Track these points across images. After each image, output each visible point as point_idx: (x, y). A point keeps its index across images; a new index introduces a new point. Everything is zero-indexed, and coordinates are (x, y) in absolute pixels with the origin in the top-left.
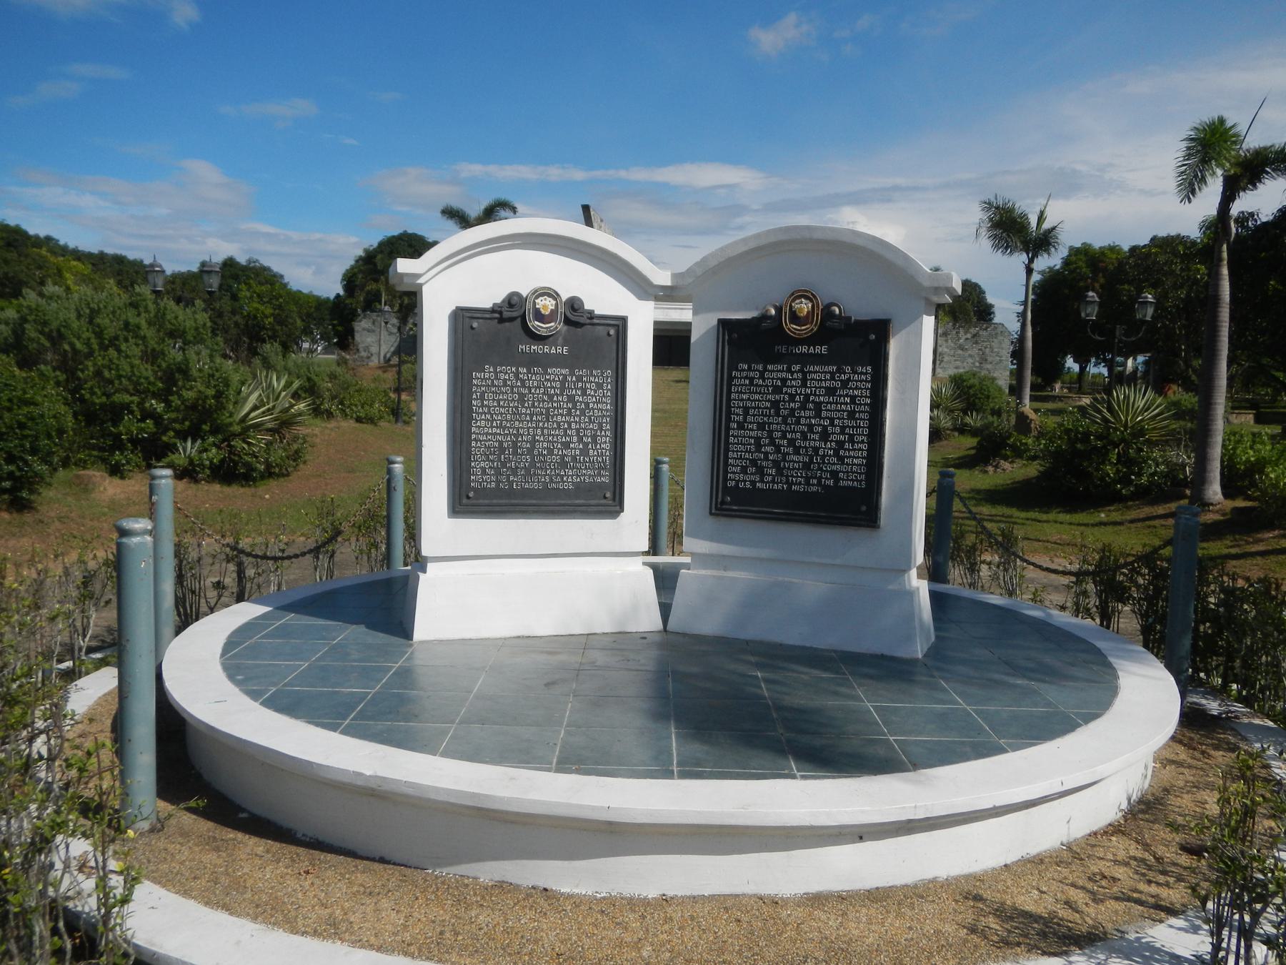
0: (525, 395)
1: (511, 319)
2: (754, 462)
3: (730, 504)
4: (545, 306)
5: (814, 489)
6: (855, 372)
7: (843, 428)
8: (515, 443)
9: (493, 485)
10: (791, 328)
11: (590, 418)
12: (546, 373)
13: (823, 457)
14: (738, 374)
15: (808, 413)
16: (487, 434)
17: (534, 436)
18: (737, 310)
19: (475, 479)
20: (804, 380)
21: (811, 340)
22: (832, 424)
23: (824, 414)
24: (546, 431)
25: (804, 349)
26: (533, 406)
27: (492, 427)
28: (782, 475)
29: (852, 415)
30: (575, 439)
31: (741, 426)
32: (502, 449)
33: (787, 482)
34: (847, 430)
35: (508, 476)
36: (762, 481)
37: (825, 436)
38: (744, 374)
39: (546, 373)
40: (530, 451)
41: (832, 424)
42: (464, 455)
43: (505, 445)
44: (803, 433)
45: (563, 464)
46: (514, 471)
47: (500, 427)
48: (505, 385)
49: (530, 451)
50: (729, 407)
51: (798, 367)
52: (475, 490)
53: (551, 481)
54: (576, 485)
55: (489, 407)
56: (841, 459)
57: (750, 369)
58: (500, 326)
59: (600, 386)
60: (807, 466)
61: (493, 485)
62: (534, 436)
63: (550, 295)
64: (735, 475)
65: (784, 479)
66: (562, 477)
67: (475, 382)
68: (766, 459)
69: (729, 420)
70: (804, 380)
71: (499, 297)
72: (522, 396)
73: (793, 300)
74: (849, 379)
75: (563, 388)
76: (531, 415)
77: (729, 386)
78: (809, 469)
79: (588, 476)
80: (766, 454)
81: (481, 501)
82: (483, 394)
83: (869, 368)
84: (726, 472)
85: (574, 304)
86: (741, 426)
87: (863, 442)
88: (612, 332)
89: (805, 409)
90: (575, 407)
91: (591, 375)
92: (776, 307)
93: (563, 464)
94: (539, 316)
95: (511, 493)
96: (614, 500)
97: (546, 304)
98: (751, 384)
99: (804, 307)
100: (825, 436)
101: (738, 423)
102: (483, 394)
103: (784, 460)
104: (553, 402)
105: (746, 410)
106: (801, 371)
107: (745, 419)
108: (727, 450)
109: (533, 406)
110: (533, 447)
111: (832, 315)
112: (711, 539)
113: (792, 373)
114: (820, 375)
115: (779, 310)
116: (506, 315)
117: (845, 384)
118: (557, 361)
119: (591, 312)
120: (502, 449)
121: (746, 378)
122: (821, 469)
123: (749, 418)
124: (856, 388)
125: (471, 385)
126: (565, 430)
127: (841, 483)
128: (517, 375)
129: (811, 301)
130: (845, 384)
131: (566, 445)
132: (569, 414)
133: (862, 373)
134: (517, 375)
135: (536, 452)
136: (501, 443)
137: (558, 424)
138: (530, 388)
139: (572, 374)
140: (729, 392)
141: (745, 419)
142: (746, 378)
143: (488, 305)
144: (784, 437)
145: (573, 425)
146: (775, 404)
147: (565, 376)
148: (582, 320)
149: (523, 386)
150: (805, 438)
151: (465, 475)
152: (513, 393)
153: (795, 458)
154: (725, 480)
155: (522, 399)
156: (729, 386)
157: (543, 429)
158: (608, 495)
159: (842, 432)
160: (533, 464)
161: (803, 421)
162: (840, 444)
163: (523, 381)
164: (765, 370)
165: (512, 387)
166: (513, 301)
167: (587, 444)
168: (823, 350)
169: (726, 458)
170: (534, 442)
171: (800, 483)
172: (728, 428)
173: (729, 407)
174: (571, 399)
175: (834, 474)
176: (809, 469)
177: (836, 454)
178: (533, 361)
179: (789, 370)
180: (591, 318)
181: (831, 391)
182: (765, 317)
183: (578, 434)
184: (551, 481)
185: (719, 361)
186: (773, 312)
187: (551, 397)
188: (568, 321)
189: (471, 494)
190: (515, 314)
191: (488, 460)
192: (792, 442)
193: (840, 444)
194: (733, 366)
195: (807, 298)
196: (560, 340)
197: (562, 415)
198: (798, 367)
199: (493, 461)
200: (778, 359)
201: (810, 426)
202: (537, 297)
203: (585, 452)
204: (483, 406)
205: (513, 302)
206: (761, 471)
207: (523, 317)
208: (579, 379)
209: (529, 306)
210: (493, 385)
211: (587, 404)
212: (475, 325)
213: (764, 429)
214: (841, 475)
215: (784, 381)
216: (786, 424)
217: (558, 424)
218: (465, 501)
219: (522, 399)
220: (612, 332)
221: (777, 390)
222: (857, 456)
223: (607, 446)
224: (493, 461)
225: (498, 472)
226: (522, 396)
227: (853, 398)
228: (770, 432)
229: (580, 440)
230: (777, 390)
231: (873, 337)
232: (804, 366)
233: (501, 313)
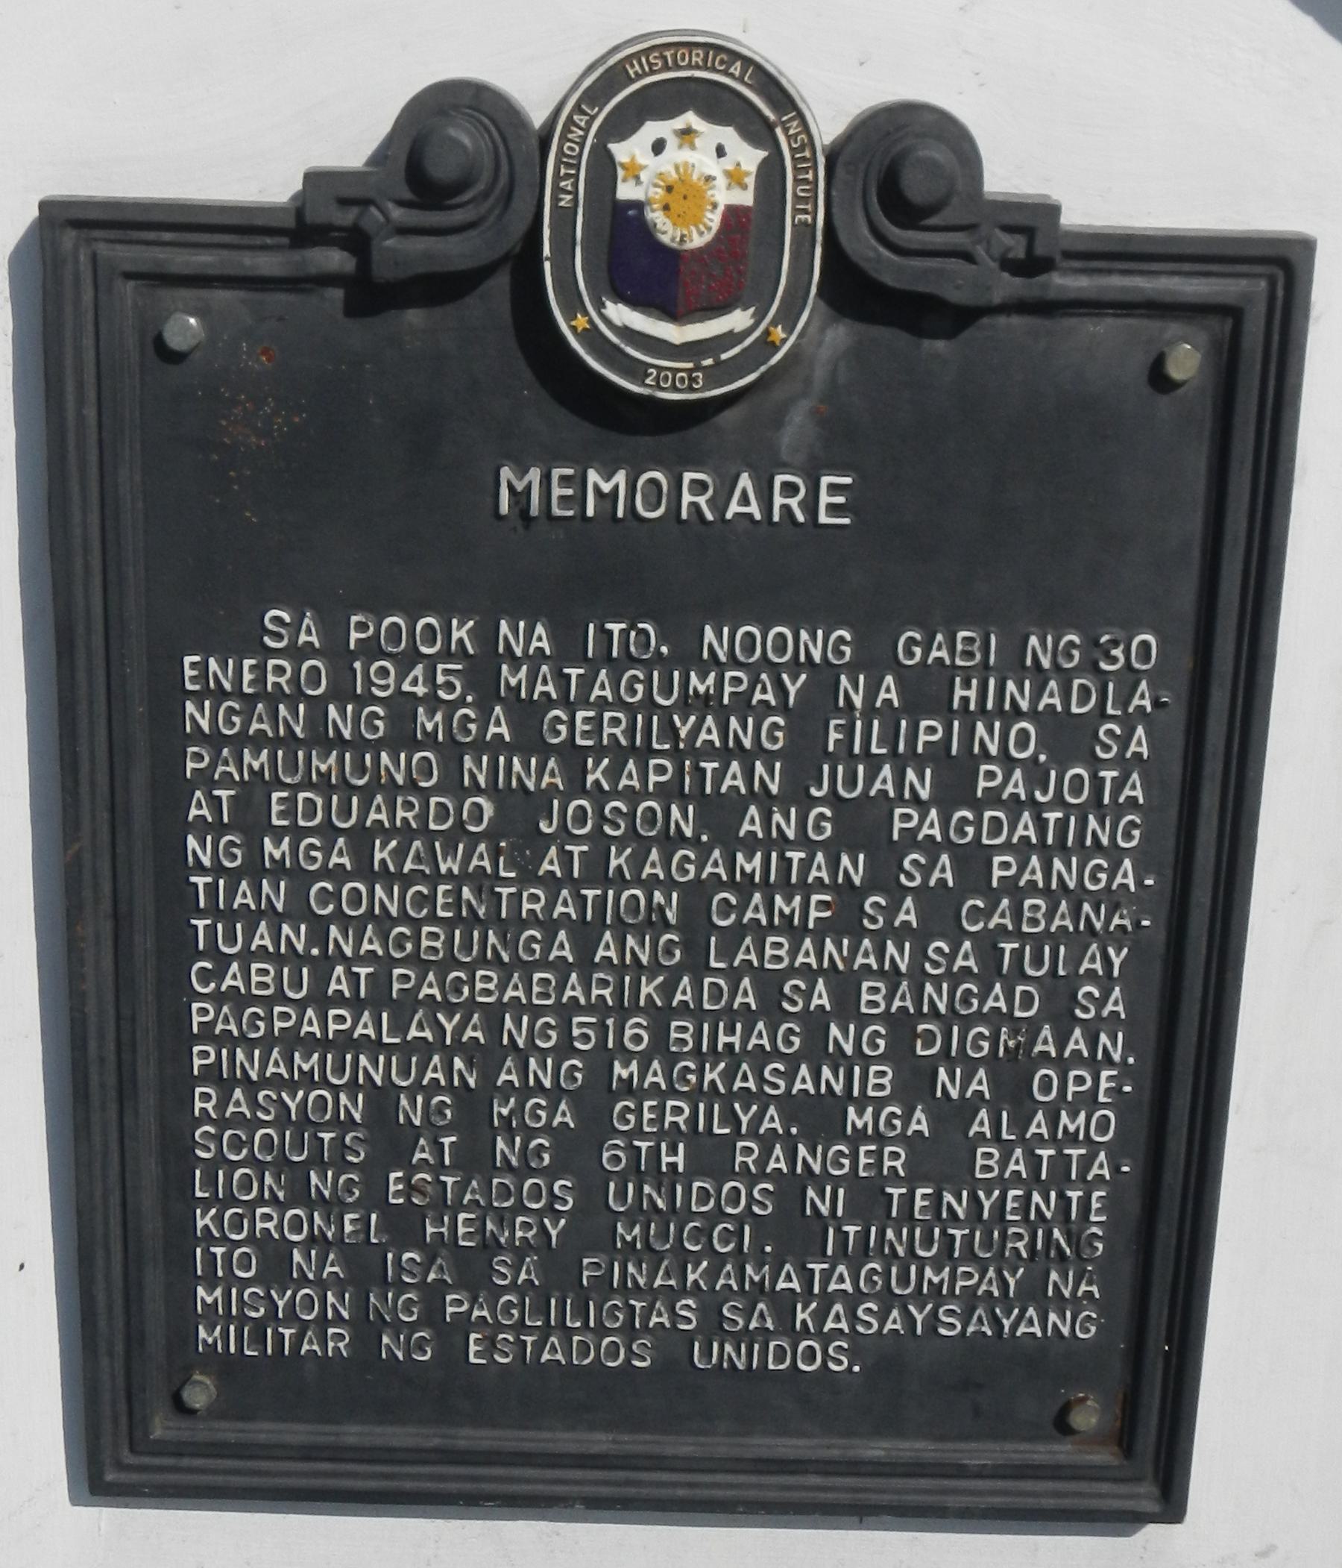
0: (540, 802)
1: (442, 288)
4: (682, 192)
8: (473, 1107)
9: (339, 1342)
11: (988, 946)
12: (689, 657)
16: (293, 1041)
17: (601, 1060)
19: (226, 1306)
24: (681, 1031)
26: (597, 871)
27: (321, 1000)
30: (881, 1078)
32: (390, 1141)
35: (433, 1296)
39: (689, 657)
40: (576, 1151)
42: (149, 1169)
43: (412, 1111)
45: (793, 1232)
46: (473, 1270)
47: (378, 998)
48: (403, 736)
49: (576, 1151)
52: (227, 1368)
53: (713, 1325)
54: (884, 1360)
55: (299, 878)
58: (359, 334)
59: (1067, 738)
61: (339, 1342)
62: (601, 1060)
63: (717, 105)
66: (783, 1306)
67: (198, 716)
71: (352, 140)
72: (521, 810)
75: (804, 757)
76: (585, 934)
79: (953, 1303)
81: (263, 1431)
82: (252, 795)
85: (904, 162)
88: (1186, 361)
90: (884, 877)
91: (1015, 664)
93: (793, 1232)
94: (636, 260)
95: (447, 1389)
96: (1125, 1438)
97: (690, 174)
102: (252, 795)
104: (733, 844)
109: (597, 871)
110: (595, 1121)
116: (401, 253)
118: (769, 573)
119: (1033, 218)
120: (390, 1141)
125: (172, 736)
126: (815, 1024)
128: (482, 671)
131: (819, 1118)
132: (846, 920)
134: (482, 671)
135: (612, 1155)
136: (382, 1099)
137: (769, 985)
138: (573, 758)
139: (873, 661)
143: (273, 185)
145: (871, 996)
147: (824, 676)
148: (956, 284)
149: (529, 739)
151: (154, 1281)
152: (454, 785)
155: (520, 822)
157: (660, 1017)
158: (1086, 1418)
160: (592, 1227)
163: (527, 713)
165: (452, 751)
166: (455, 153)
167: (967, 1109)
170: (597, 1097)
174: (862, 825)
178: (591, 576)
180: (1033, 266)
183: (900, 1052)
184: (713, 1325)
187: (720, 816)
188: (849, 289)
189: (199, 1394)
190: (456, 252)
191: (299, 1194)
196: (798, 427)
197: (795, 931)
199: (333, 1208)
202: (623, 125)
203: (943, 1158)
204: (255, 869)
205: (442, 168)
207: (525, 260)
208: (927, 692)
209: (563, 186)
210: (321, 739)
211: (973, 861)
212: (186, 328)
217: (769, 985)
218: (161, 1427)
219: (520, 822)
220: (1186, 361)
223: (1100, 1127)
224: (333, 1208)
225: (364, 1270)
226: (521, 810)
229: (915, 1084)
233: (357, 241)
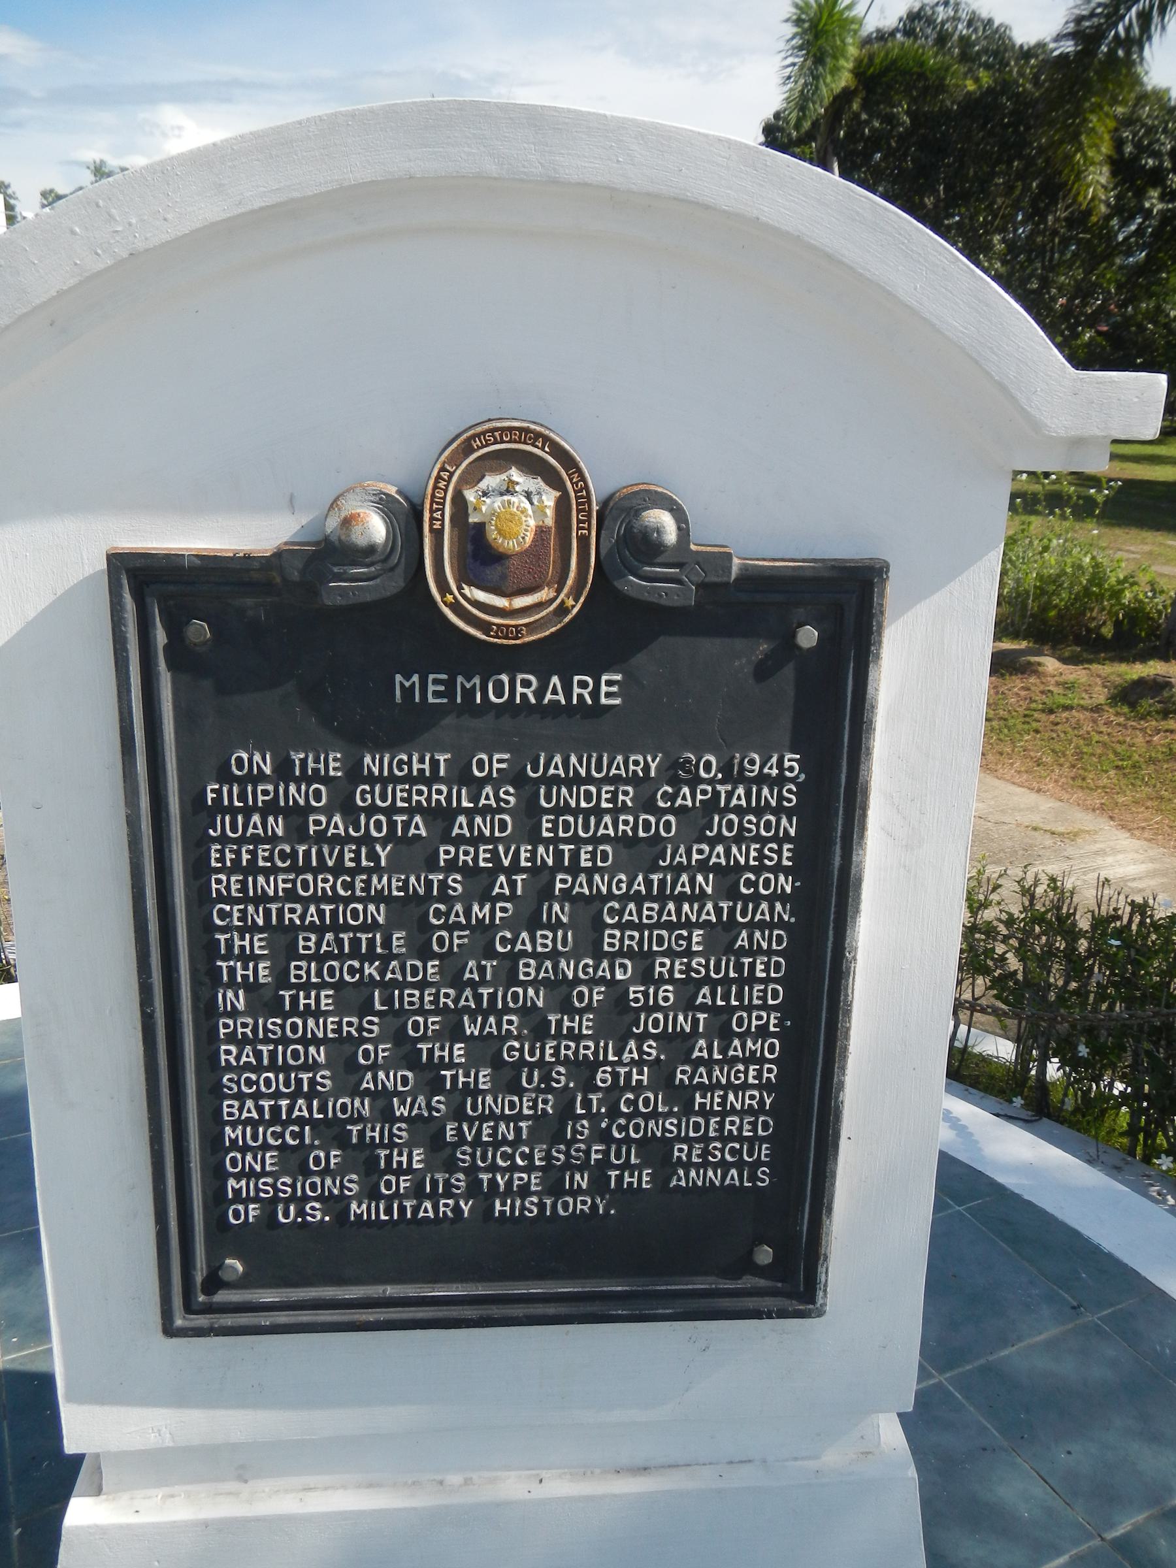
2: (333, 1131)
3: (243, 1283)
5: (582, 1205)
6: (732, 775)
7: (688, 987)
10: (467, 603)
13: (615, 1090)
14: (231, 795)
15: (545, 940)
18: (195, 503)
20: (530, 811)
21: (559, 653)
22: (646, 976)
23: (610, 940)
25: (525, 687)
28: (451, 1166)
29: (722, 936)
31: (265, 1002)
33: (474, 1188)
34: (704, 995)
36: (373, 1194)
37: (618, 1017)
38: (263, 793)
41: (646, 976)
44: (527, 1011)
50: (203, 929)
51: (499, 761)
56: (681, 1097)
57: (284, 771)
60: (552, 1129)
64: (256, 1182)
65: (460, 1180)
68: (387, 1116)
69: (208, 979)
70: (530, 811)
73: (473, 476)
74: (711, 806)
77: (197, 846)
78: (558, 1137)
80: (382, 1096)
83: (791, 760)
84: (217, 1175)
86: (265, 1002)
87: (763, 1032)
89: (534, 924)
92: (385, 505)
98: (298, 833)
99: (519, 510)
100: (618, 1017)
101: (252, 987)
103: (459, 1115)
105: (284, 939)
106: (517, 778)
107: (281, 978)
108: (213, 1093)
111: (645, 546)
112: (179, 1399)
113: (476, 786)
114: (600, 791)
115: (407, 516)
117: (696, 823)
121: (271, 808)
122: (605, 1137)
123: (297, 970)
124: (739, 839)
127: (680, 1180)
129: (553, 480)
130: (696, 823)
133: (762, 779)
140: (199, 870)
141: (281, 978)
142: (271, 808)
144: (454, 1032)
146: (410, 911)
150: (539, 1031)
153: (502, 1105)
154: (217, 1199)
156: (197, 846)
159: (688, 1004)
161: (527, 969)
162: (677, 1044)
164: (355, 774)
168: (608, 688)
169: (213, 1121)
171: (525, 1191)
172: (208, 1012)
173: (203, 929)
175: (657, 1152)
176: (558, 1137)
177: (663, 1078)
179: (462, 776)
181: (640, 852)
182: (329, 553)
185: (139, 743)
186: (376, 528)
192: (486, 1050)
193: (677, 1044)
194: (206, 760)
195: (533, 466)
198: (499, 761)
200: (407, 726)
201: (561, 990)
206: (367, 1163)
213: (366, 1009)
214: (680, 1151)
215: (441, 816)
216: (458, 983)
221: (414, 854)
222: (741, 1084)
227: (728, 874)
228: (395, 1014)
230: (414, 854)
231: (808, 637)
232: (523, 752)
